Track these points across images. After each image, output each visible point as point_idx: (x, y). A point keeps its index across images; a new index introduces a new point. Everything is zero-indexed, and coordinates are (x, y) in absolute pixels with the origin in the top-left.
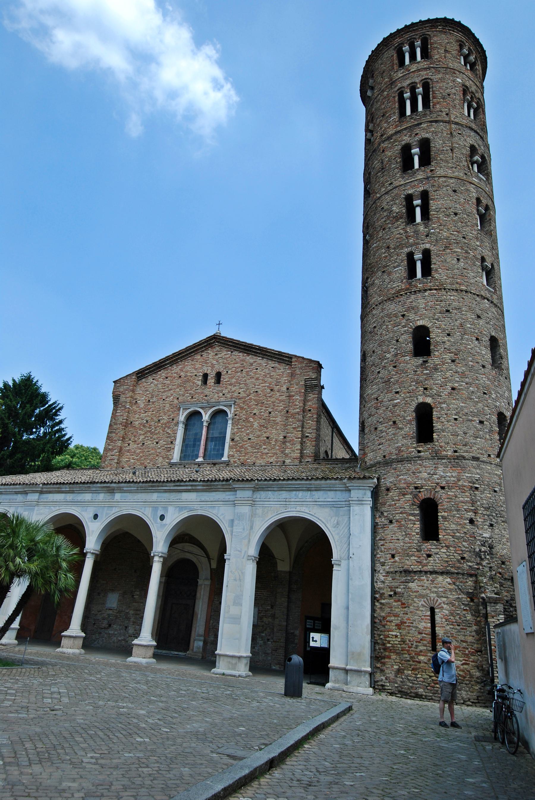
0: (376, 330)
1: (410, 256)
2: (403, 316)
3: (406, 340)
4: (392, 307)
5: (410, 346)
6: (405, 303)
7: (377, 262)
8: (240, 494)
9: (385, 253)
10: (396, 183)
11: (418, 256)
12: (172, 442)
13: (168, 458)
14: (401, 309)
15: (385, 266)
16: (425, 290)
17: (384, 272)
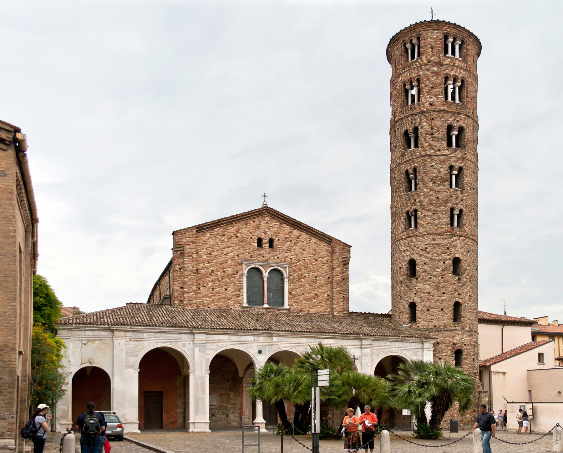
0: (428, 250)
1: (452, 210)
2: (448, 248)
3: (450, 264)
4: (441, 240)
5: (451, 268)
6: (449, 240)
7: (427, 204)
8: (364, 342)
9: (435, 201)
10: (443, 152)
11: (457, 212)
12: (239, 290)
13: (239, 303)
14: (447, 244)
15: (434, 210)
16: (460, 236)
17: (434, 214)
